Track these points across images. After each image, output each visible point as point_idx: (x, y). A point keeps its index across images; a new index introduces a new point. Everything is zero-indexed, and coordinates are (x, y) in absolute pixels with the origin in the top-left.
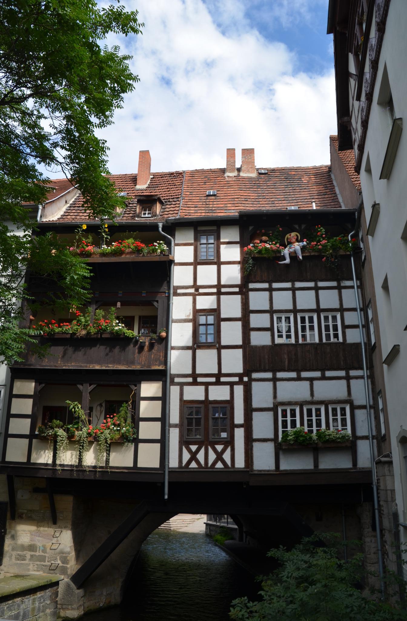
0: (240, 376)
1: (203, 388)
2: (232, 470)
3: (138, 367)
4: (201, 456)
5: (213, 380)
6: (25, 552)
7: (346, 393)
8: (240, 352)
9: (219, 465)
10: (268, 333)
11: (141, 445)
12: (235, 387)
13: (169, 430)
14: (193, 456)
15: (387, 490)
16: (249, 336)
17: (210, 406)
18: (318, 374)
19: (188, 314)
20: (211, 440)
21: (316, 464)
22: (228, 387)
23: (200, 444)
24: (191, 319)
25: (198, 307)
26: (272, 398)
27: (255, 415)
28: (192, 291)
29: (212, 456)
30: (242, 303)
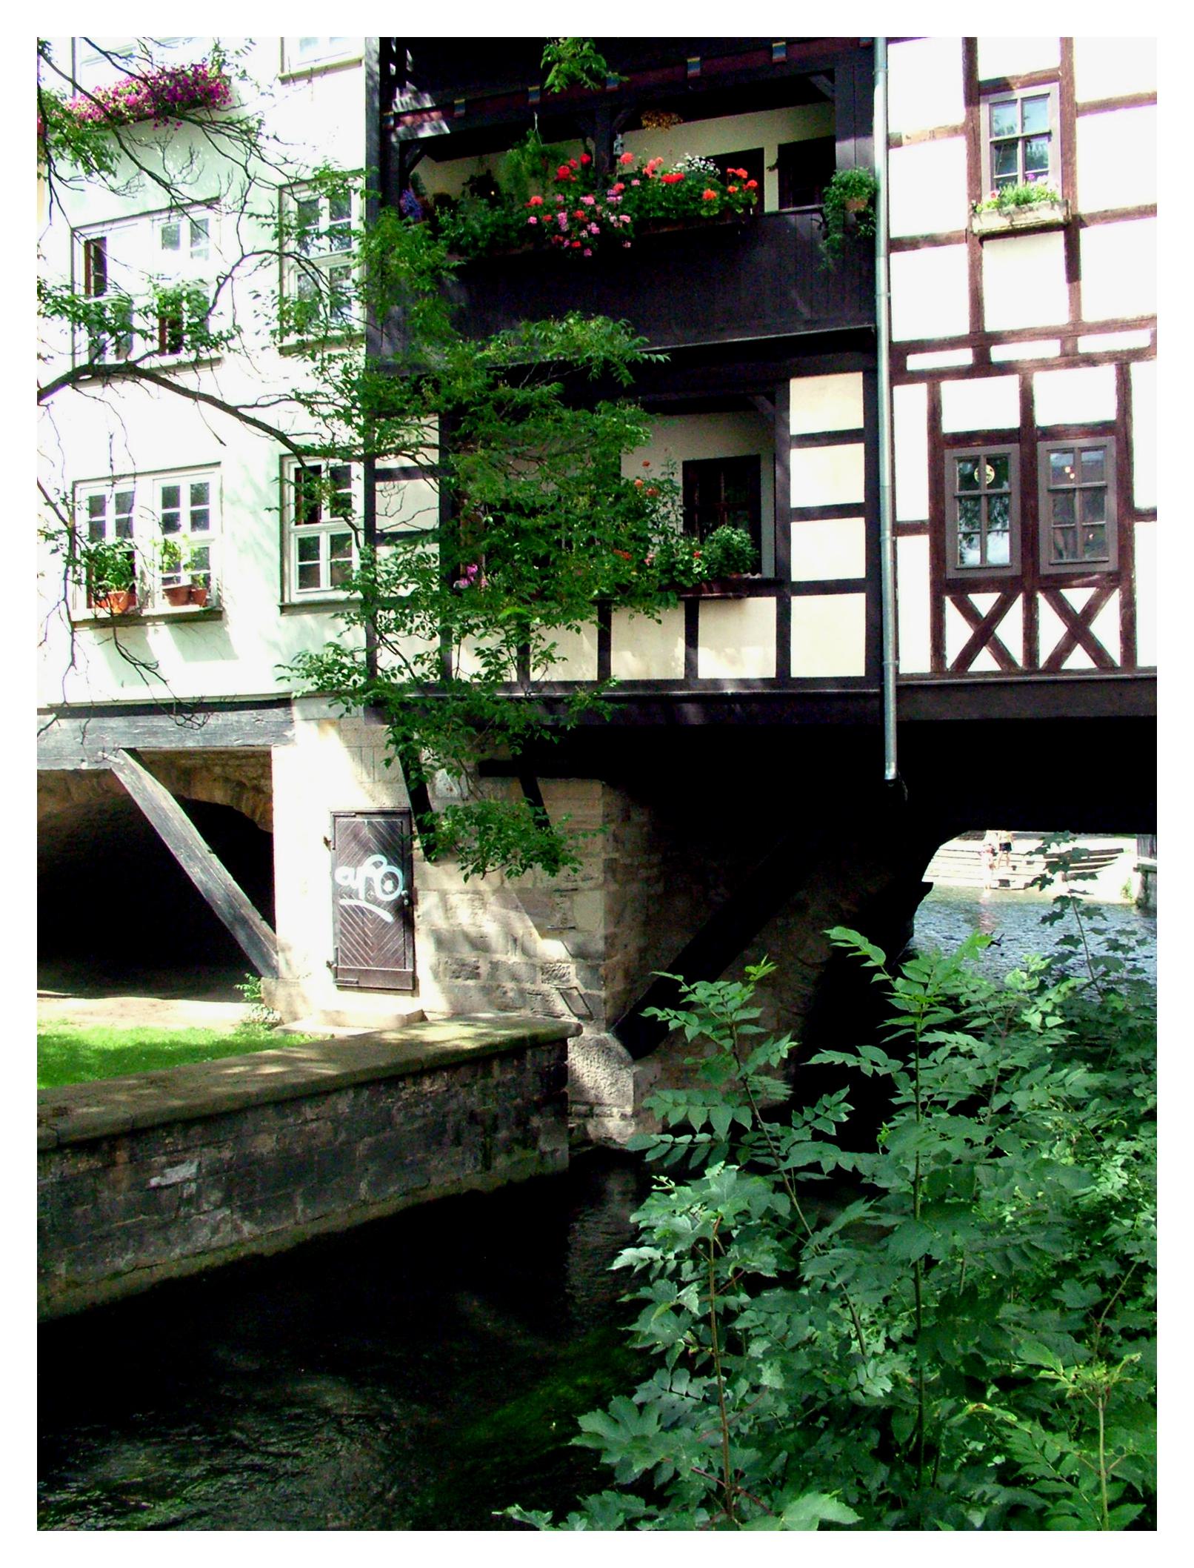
4: (1010, 631)
5: (1051, 349)
9: (1079, 660)
11: (798, 603)
13: (894, 544)
14: (984, 632)
17: (1042, 446)
20: (1045, 570)
29: (1052, 630)
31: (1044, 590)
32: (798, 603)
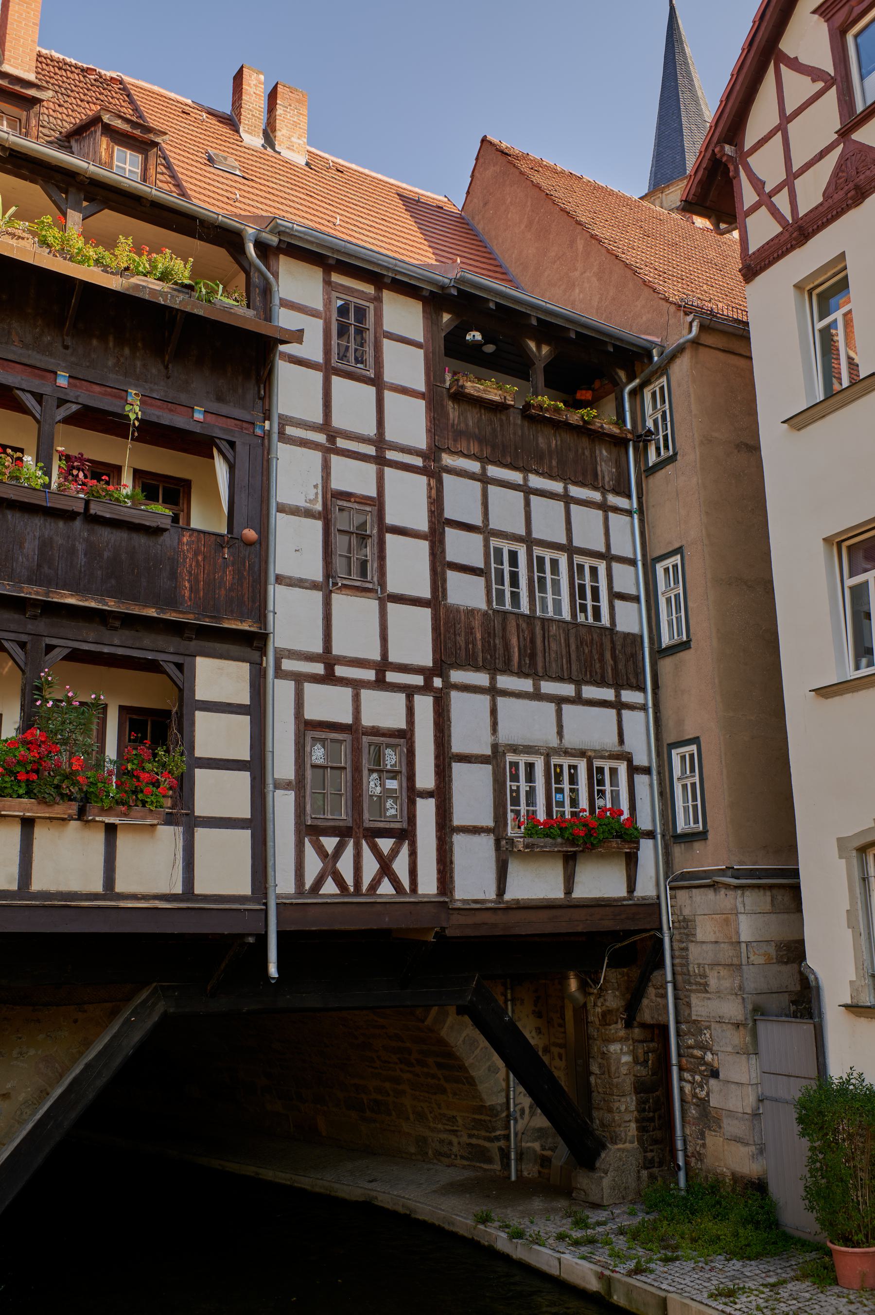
0: (428, 673)
1: (348, 692)
2: (412, 900)
3: (191, 616)
7: (616, 739)
8: (426, 613)
9: (386, 888)
10: (481, 581)
11: (200, 833)
12: (417, 698)
15: (739, 942)
16: (444, 581)
17: (365, 739)
18: (567, 690)
19: (312, 497)
20: (367, 824)
21: (569, 891)
22: (401, 697)
23: (343, 833)
24: (319, 513)
25: (336, 484)
26: (490, 734)
27: (456, 767)
28: (321, 438)
29: (371, 867)
30: (429, 497)
31: (365, 837)
32: (200, 833)
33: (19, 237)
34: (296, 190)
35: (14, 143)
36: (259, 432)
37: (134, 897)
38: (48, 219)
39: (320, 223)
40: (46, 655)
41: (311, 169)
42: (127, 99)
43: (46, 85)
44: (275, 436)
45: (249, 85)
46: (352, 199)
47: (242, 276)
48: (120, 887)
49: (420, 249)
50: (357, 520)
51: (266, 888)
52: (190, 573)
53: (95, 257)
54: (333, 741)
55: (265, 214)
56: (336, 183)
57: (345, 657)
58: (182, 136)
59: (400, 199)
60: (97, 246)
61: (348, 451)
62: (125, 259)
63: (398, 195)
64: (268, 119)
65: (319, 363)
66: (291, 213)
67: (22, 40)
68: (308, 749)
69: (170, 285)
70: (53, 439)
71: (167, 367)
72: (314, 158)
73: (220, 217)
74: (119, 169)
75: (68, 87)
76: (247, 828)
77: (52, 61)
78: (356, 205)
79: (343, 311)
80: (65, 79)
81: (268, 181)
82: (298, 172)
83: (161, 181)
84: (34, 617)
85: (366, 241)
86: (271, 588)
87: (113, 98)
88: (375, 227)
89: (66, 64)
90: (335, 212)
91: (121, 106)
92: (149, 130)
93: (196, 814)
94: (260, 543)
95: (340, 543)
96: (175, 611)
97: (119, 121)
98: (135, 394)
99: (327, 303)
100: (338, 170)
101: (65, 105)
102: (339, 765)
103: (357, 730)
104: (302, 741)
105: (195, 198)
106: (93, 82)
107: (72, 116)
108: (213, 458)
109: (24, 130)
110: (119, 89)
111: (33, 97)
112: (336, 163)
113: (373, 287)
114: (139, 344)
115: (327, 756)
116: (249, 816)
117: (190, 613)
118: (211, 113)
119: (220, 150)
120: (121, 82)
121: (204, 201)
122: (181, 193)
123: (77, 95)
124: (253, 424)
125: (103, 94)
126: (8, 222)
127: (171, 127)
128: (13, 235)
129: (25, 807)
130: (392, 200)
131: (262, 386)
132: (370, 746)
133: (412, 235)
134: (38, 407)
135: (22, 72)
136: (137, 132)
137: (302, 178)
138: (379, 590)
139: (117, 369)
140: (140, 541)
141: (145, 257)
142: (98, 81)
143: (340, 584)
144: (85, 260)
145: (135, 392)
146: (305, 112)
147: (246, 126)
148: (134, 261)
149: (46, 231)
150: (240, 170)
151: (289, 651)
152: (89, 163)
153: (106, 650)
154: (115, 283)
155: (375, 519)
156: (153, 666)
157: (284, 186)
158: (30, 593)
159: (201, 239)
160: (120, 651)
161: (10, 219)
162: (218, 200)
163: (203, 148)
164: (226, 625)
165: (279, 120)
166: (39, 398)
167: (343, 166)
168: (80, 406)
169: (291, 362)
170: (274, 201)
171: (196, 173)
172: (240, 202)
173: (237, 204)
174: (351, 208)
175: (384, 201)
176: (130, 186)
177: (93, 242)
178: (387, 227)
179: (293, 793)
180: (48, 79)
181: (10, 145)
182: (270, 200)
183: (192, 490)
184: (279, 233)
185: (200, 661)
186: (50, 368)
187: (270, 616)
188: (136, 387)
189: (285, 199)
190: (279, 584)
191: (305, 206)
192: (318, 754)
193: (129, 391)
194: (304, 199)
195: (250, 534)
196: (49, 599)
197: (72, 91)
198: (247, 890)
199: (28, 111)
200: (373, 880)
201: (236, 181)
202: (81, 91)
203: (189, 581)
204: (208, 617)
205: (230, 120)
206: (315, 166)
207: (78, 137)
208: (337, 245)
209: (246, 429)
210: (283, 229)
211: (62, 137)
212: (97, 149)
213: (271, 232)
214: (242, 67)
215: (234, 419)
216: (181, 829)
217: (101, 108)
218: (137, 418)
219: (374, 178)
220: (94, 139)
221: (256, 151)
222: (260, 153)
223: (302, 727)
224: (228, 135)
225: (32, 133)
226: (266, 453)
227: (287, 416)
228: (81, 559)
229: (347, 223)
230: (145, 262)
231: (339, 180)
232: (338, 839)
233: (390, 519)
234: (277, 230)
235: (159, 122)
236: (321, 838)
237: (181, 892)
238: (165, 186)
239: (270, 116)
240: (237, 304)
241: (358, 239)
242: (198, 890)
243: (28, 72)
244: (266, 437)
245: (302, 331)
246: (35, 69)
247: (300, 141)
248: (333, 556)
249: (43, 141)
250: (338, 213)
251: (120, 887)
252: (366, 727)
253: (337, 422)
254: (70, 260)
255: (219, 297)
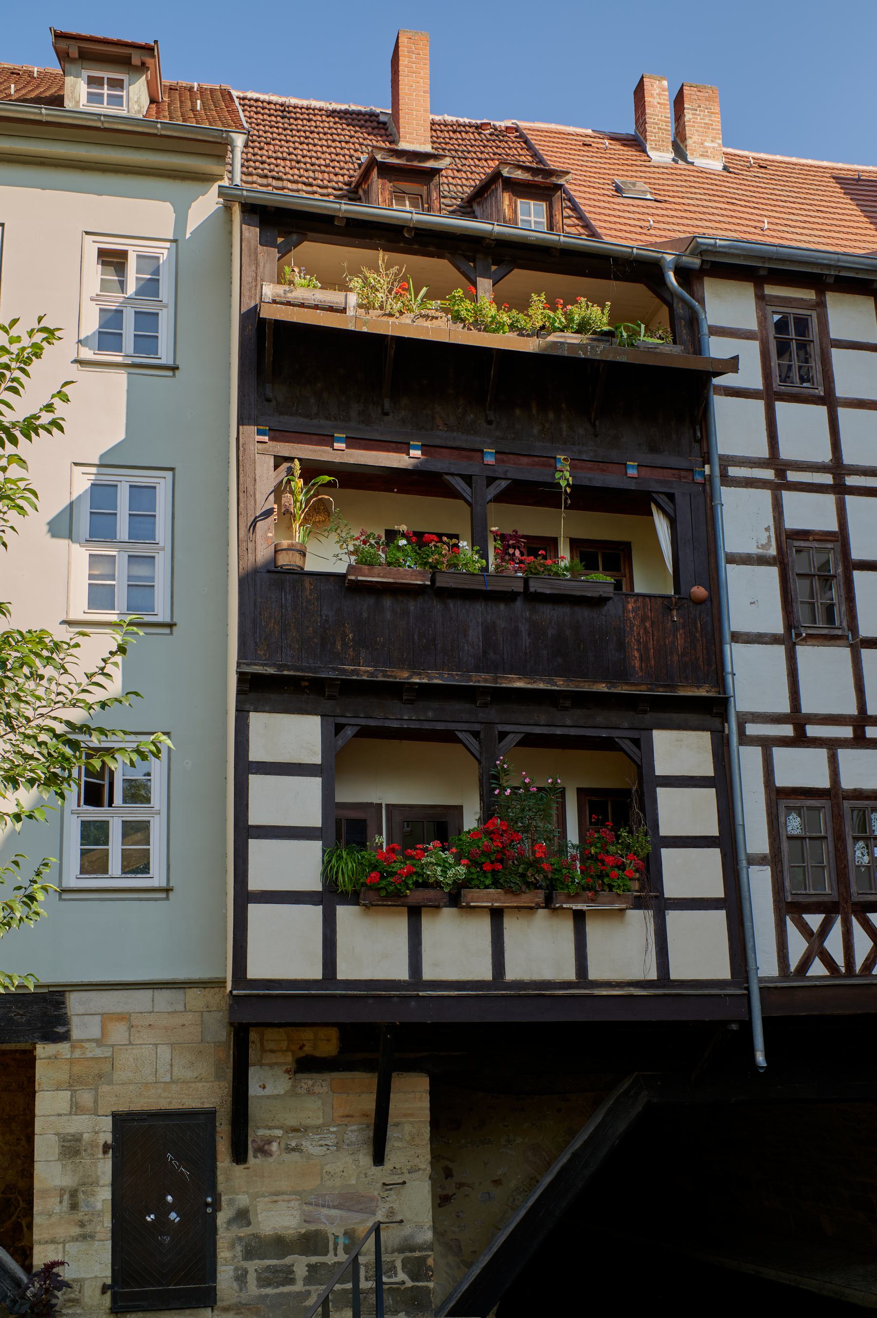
1: (822, 754)
3: (644, 687)
4: (834, 944)
5: (847, 732)
6: (288, 1260)
11: (672, 916)
17: (847, 804)
19: (764, 541)
20: (855, 898)
23: (829, 909)
24: (774, 558)
25: (790, 524)
28: (768, 474)
33: (433, 318)
34: (715, 201)
35: (418, 221)
36: (699, 479)
37: (608, 984)
38: (459, 293)
39: (745, 232)
40: (499, 743)
41: (730, 172)
42: (524, 146)
43: (443, 153)
44: (717, 480)
45: (652, 96)
46: (780, 195)
47: (665, 309)
48: (593, 974)
49: (865, 235)
50: (818, 560)
51: (747, 972)
52: (638, 641)
53: (509, 322)
54: (809, 808)
55: (682, 236)
56: (760, 182)
57: (816, 715)
58: (586, 171)
59: (837, 183)
60: (510, 310)
61: (801, 483)
62: (540, 317)
63: (834, 178)
64: (676, 129)
65: (759, 390)
66: (712, 228)
67: (415, 112)
68: (782, 819)
69: (589, 336)
70: (486, 519)
71: (594, 425)
72: (732, 159)
73: (635, 250)
74: (525, 224)
75: (465, 148)
76: (721, 909)
77: (446, 126)
78: (785, 201)
79: (781, 326)
80: (460, 142)
81: (683, 198)
82: (715, 180)
83: (569, 226)
84: (485, 705)
85: (800, 241)
86: (727, 648)
87: (510, 148)
88: (809, 222)
89: (459, 125)
90: (761, 215)
91: (520, 155)
92: (551, 173)
93: (666, 896)
94: (711, 600)
95: (800, 588)
96: (627, 684)
97: (520, 172)
98: (564, 459)
99: (762, 320)
100: (761, 167)
101: (464, 169)
102: (818, 834)
103: (836, 794)
104: (775, 811)
105: (606, 235)
106: (489, 137)
107: (471, 179)
108: (651, 514)
109: (426, 206)
110: (516, 137)
111: (431, 168)
112: (758, 159)
113: (813, 292)
114: (564, 406)
115: (804, 825)
116: (723, 896)
117: (642, 684)
118: (614, 138)
119: (627, 176)
120: (517, 129)
121: (616, 237)
122: (591, 233)
123: (474, 156)
124: (692, 470)
125: (500, 147)
126: (421, 305)
127: (573, 164)
128: (427, 317)
129: (491, 897)
130: (827, 186)
131: (698, 427)
132: (852, 811)
133: (854, 221)
134: (468, 490)
135: (418, 145)
136: (539, 179)
137: (721, 186)
138: (850, 635)
139: (543, 436)
140: (583, 614)
141: (560, 312)
142: (493, 134)
143: (804, 635)
144: (500, 327)
145: (563, 457)
146: (717, 109)
147: (653, 143)
148: (549, 317)
149: (458, 305)
150: (651, 193)
151: (752, 714)
152: (493, 224)
153: (559, 731)
154: (531, 345)
155: (839, 557)
156: (608, 744)
157: (701, 200)
158: (479, 681)
159: (617, 279)
160: (573, 732)
161: (422, 301)
162: (631, 232)
163: (609, 179)
164: (681, 693)
165: (689, 126)
166: (468, 479)
167: (766, 160)
168: (509, 481)
169: (726, 395)
170: (691, 219)
171: (605, 208)
172: (655, 228)
173: (651, 232)
174: (779, 206)
175: (817, 190)
176: (537, 239)
177: (505, 307)
178: (824, 218)
179: (769, 868)
180: (444, 146)
181: (414, 224)
182: (687, 218)
183: (633, 553)
184: (701, 253)
185: (655, 733)
186: (477, 446)
187: (729, 678)
188: (563, 451)
189: (704, 213)
190: (736, 642)
191: (727, 216)
192: (794, 825)
193: (558, 456)
194: (725, 209)
195: (699, 591)
196: (498, 685)
197: (469, 152)
198: (725, 974)
199: (428, 184)
200: (867, 959)
201: (648, 207)
202: (478, 149)
203: (638, 650)
204: (661, 686)
205: (635, 140)
206: (734, 168)
207: (480, 199)
208: (767, 251)
209: (684, 477)
210: (705, 247)
211: (464, 203)
212: (499, 207)
213: (692, 254)
214: (642, 77)
215: (671, 468)
216: (651, 912)
217: (500, 163)
218: (568, 485)
219: (803, 165)
220: (496, 197)
221: (666, 168)
222: (672, 168)
223: (774, 796)
224: (634, 158)
225: (435, 207)
226: (708, 500)
227: (728, 456)
228: (525, 640)
229: (777, 224)
230: (560, 317)
231: (763, 178)
232: (824, 916)
233: (857, 553)
234: (699, 250)
235: (559, 162)
236: (804, 916)
237: (656, 978)
238: (573, 230)
239: (678, 125)
240: (662, 342)
241: (791, 240)
242: (674, 976)
243: (424, 144)
244: (707, 483)
245: (736, 358)
246: (430, 139)
247: (714, 144)
248: (794, 604)
249: (445, 212)
250: (765, 216)
251: (593, 974)
252: (847, 791)
253: (786, 452)
254: (485, 330)
255: (642, 338)
